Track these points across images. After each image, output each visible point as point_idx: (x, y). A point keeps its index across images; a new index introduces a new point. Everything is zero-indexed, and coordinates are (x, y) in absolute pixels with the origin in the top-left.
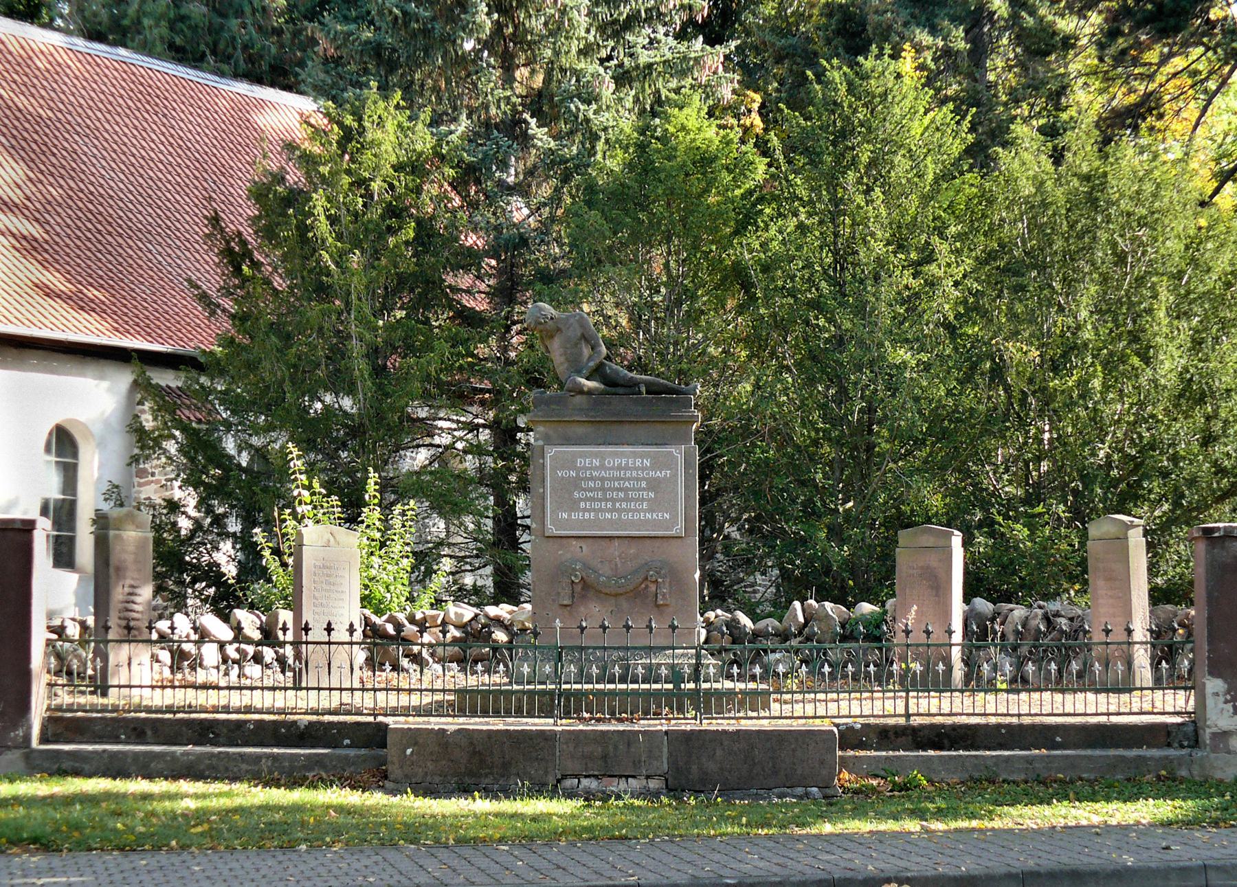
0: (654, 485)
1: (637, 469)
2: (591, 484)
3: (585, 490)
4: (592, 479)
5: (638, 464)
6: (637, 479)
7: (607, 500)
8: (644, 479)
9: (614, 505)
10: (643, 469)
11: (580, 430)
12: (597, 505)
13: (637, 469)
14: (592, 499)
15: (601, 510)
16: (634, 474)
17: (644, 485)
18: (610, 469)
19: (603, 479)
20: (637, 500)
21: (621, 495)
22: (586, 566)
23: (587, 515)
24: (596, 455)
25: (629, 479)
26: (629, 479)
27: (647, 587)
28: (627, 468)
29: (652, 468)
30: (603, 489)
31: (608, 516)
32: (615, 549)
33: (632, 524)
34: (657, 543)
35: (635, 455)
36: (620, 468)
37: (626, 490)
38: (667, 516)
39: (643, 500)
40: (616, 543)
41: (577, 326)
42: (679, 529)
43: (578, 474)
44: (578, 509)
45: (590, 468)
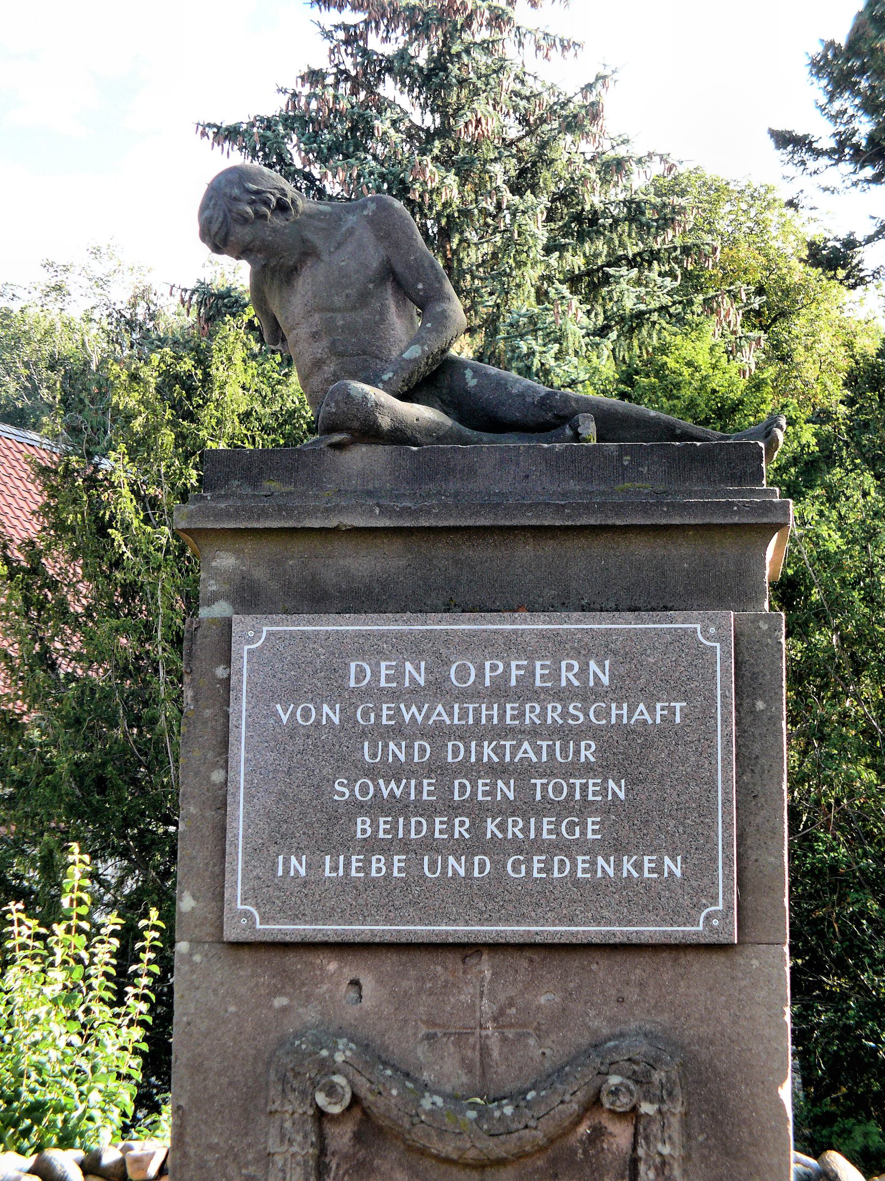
0: (626, 752)
1: (561, 695)
2: (396, 750)
3: (372, 772)
4: (398, 731)
5: (568, 677)
6: (564, 733)
7: (453, 809)
8: (592, 732)
9: (477, 828)
10: (587, 695)
11: (361, 563)
12: (414, 828)
13: (561, 695)
14: (398, 807)
15: (429, 845)
16: (553, 714)
17: (588, 752)
18: (464, 696)
19: (438, 734)
20: (560, 809)
21: (506, 790)
22: (372, 1055)
23: (378, 864)
24: (414, 647)
25: (534, 733)
26: (534, 733)
27: (598, 1133)
28: (526, 692)
29: (620, 691)
30: (438, 769)
31: (456, 866)
32: (479, 989)
33: (541, 897)
34: (638, 969)
35: (557, 646)
36: (500, 692)
37: (522, 773)
38: (673, 867)
39: (585, 807)
40: (485, 966)
41: (367, 236)
42: (714, 915)
43: (348, 718)
44: (346, 844)
45: (394, 695)
